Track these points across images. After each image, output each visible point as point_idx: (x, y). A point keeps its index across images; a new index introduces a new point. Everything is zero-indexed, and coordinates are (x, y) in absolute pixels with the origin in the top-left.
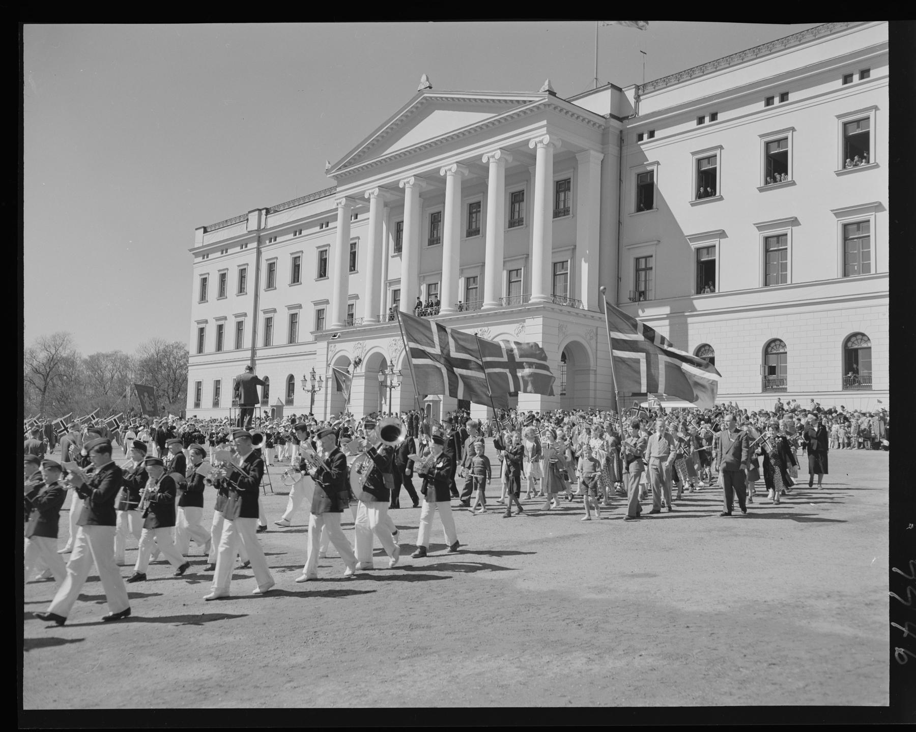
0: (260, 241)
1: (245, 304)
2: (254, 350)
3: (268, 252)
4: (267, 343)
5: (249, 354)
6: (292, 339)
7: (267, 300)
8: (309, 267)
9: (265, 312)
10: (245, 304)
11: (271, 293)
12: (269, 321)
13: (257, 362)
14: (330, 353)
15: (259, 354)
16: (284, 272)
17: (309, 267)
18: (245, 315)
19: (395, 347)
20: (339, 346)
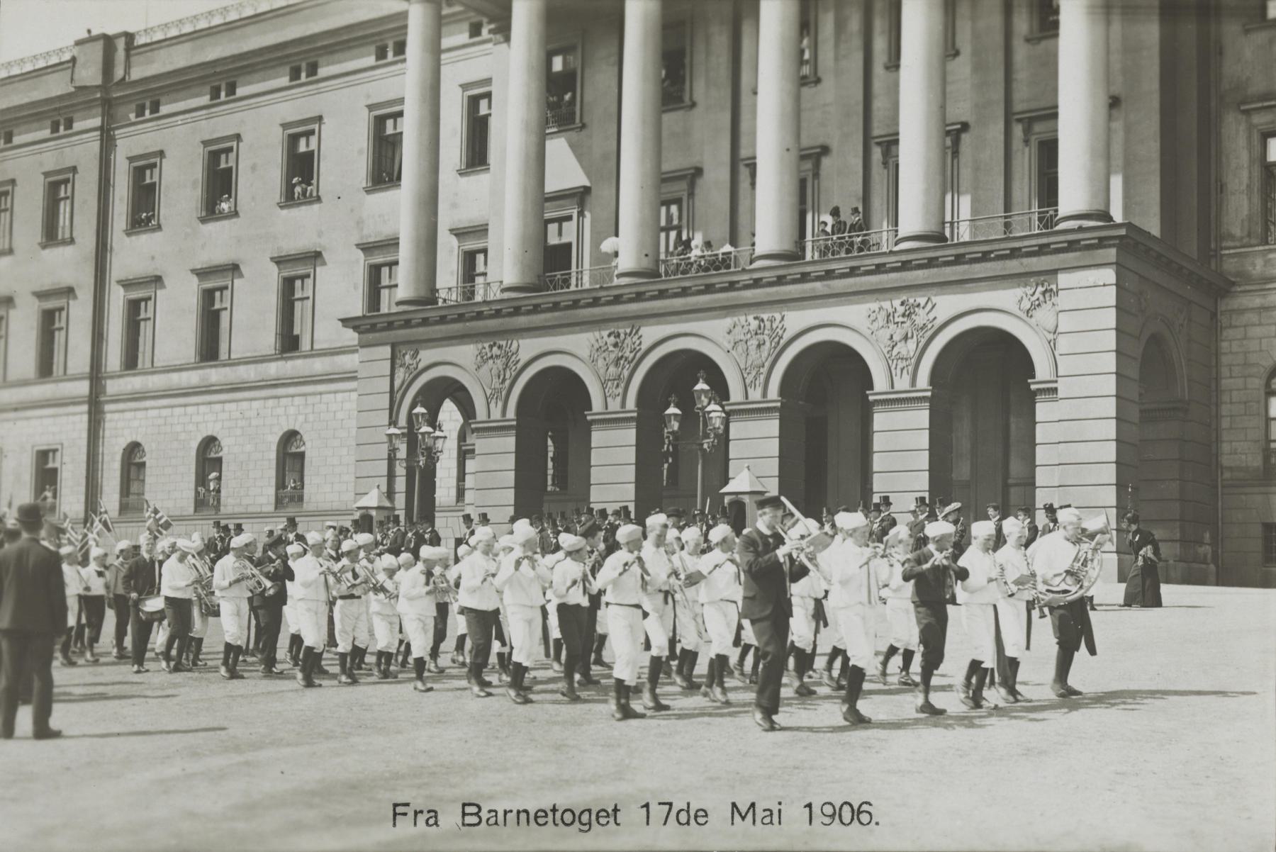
0: (108, 106)
1: (68, 264)
2: (96, 375)
3: (132, 142)
4: (131, 362)
5: (83, 388)
6: (209, 349)
7: (132, 254)
8: (259, 173)
9: (127, 284)
10: (68, 264)
11: (145, 241)
12: (134, 307)
13: (107, 407)
14: (400, 375)
15: (112, 387)
16: (181, 185)
17: (259, 173)
18: (69, 292)
19: (616, 353)
20: (427, 356)
